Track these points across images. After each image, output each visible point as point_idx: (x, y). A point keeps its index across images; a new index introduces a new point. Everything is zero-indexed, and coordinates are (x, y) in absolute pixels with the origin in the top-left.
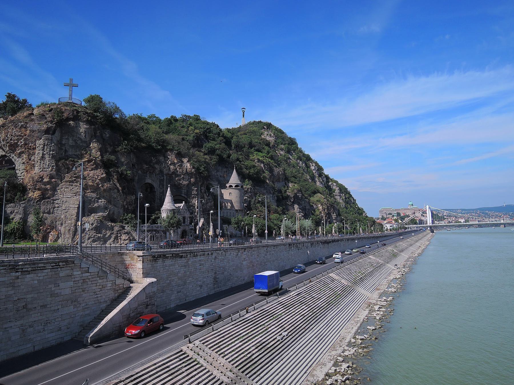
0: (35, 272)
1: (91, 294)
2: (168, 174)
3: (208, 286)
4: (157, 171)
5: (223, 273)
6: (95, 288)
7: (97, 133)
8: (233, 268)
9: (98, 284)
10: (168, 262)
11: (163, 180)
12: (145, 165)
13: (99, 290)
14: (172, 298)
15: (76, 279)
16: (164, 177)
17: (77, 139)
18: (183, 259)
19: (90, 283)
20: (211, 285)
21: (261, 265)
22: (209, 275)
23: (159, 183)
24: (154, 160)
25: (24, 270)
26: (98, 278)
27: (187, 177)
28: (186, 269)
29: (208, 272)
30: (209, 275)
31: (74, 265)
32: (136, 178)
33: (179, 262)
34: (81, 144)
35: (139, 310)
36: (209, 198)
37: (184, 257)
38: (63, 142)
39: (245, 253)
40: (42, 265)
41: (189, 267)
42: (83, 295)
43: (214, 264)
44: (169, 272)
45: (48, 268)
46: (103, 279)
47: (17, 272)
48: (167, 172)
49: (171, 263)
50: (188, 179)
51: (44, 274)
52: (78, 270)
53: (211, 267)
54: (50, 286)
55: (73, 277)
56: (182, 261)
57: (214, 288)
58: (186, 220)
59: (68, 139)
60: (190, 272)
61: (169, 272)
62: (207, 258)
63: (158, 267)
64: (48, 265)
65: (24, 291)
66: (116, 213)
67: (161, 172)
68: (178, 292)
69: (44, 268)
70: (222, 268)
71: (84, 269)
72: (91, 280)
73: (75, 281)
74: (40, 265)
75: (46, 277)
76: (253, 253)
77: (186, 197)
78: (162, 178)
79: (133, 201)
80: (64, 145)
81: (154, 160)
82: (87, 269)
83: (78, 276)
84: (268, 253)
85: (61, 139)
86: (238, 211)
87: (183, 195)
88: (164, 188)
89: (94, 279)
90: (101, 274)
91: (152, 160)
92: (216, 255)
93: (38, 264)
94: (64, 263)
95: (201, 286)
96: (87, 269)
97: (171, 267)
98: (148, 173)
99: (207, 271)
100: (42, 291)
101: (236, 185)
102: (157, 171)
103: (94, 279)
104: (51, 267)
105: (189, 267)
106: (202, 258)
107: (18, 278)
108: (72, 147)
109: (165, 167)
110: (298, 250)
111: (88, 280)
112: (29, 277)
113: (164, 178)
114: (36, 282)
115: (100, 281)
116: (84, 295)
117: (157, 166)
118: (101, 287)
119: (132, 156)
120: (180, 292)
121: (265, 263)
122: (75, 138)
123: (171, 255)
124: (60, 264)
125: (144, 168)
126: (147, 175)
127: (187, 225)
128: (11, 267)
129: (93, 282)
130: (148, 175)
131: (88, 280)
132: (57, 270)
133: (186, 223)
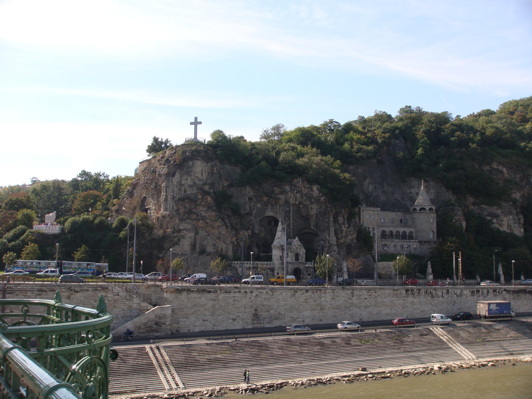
0: (82, 292)
1: (121, 310)
2: (295, 205)
3: (245, 320)
4: (281, 202)
5: (268, 311)
6: (123, 306)
7: (214, 170)
8: (285, 308)
9: (126, 304)
10: (193, 295)
11: (289, 212)
12: (266, 197)
13: (127, 308)
14: (196, 324)
15: (109, 299)
16: (290, 208)
17: (195, 178)
18: (211, 294)
19: (120, 303)
20: (248, 320)
21: (338, 309)
22: (246, 311)
23: (284, 215)
24: (277, 190)
25: (75, 290)
26: (126, 300)
27: (316, 206)
28: (215, 303)
29: (245, 308)
30: (246, 311)
31: (107, 290)
32: (254, 212)
33: (206, 296)
34: (198, 183)
35: (149, 325)
36: (350, 229)
37: (213, 292)
38: (183, 183)
39: (306, 294)
40: (87, 288)
41: (218, 301)
42: (114, 310)
43: (254, 302)
44: (194, 303)
45: (90, 290)
46: (130, 301)
47: (72, 291)
48: (293, 202)
49: (198, 296)
50: (317, 209)
51: (88, 294)
52: (111, 293)
53: (249, 303)
54: (91, 301)
55: (107, 297)
56: (211, 296)
57: (254, 324)
58: (300, 258)
59: (187, 179)
60: (220, 306)
61: (194, 303)
62: (244, 295)
63: (182, 298)
64: (90, 288)
65: (76, 302)
66: (224, 249)
67: (287, 202)
68: (204, 321)
69: (88, 290)
70: (266, 307)
71: (115, 293)
72: (120, 301)
73: (108, 300)
74: (85, 288)
75: (89, 296)
76: (323, 295)
77: (315, 229)
78: (288, 209)
79: (247, 236)
80: (184, 185)
81: (277, 190)
82: (118, 293)
83: (111, 297)
84: (354, 297)
85: (181, 181)
86: (423, 243)
87: (312, 228)
88: (290, 220)
89: (123, 301)
90: (128, 297)
91: (274, 190)
92: (257, 293)
93: (84, 287)
94: (101, 288)
95: (234, 320)
96: (118, 293)
97: (197, 299)
98: (269, 205)
99: (244, 307)
100: (86, 303)
101: (420, 207)
102: (281, 202)
103: (123, 301)
104: (92, 290)
105: (218, 301)
106: (237, 295)
107: (72, 294)
108: (190, 186)
109: (291, 196)
110: (433, 297)
111: (118, 301)
112: (78, 295)
113: (290, 209)
114: (83, 298)
115: (127, 302)
116: (115, 310)
117: (282, 197)
118: (128, 306)
119: (247, 189)
120: (207, 321)
121: (346, 307)
122: (193, 178)
123: (197, 290)
124: (98, 288)
125: (264, 200)
126: (268, 207)
127: (301, 263)
128: (68, 288)
129: (122, 303)
130: (269, 207)
131: (118, 301)
132: (96, 292)
133: (300, 261)
